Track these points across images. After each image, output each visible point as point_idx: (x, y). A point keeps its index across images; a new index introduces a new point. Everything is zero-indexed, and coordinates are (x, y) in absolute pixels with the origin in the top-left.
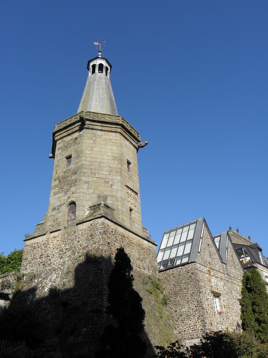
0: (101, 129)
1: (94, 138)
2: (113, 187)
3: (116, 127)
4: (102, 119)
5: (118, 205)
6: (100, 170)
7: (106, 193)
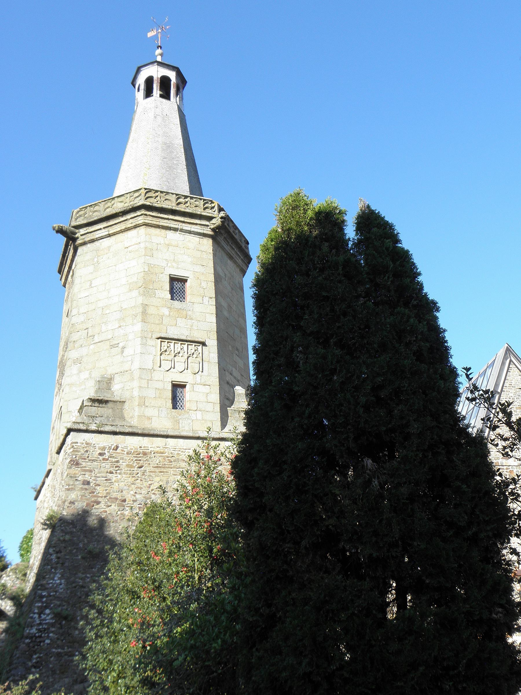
0: (107, 233)
1: (96, 260)
2: (126, 352)
3: (136, 215)
4: (108, 210)
5: (133, 389)
6: (103, 325)
7: (110, 371)
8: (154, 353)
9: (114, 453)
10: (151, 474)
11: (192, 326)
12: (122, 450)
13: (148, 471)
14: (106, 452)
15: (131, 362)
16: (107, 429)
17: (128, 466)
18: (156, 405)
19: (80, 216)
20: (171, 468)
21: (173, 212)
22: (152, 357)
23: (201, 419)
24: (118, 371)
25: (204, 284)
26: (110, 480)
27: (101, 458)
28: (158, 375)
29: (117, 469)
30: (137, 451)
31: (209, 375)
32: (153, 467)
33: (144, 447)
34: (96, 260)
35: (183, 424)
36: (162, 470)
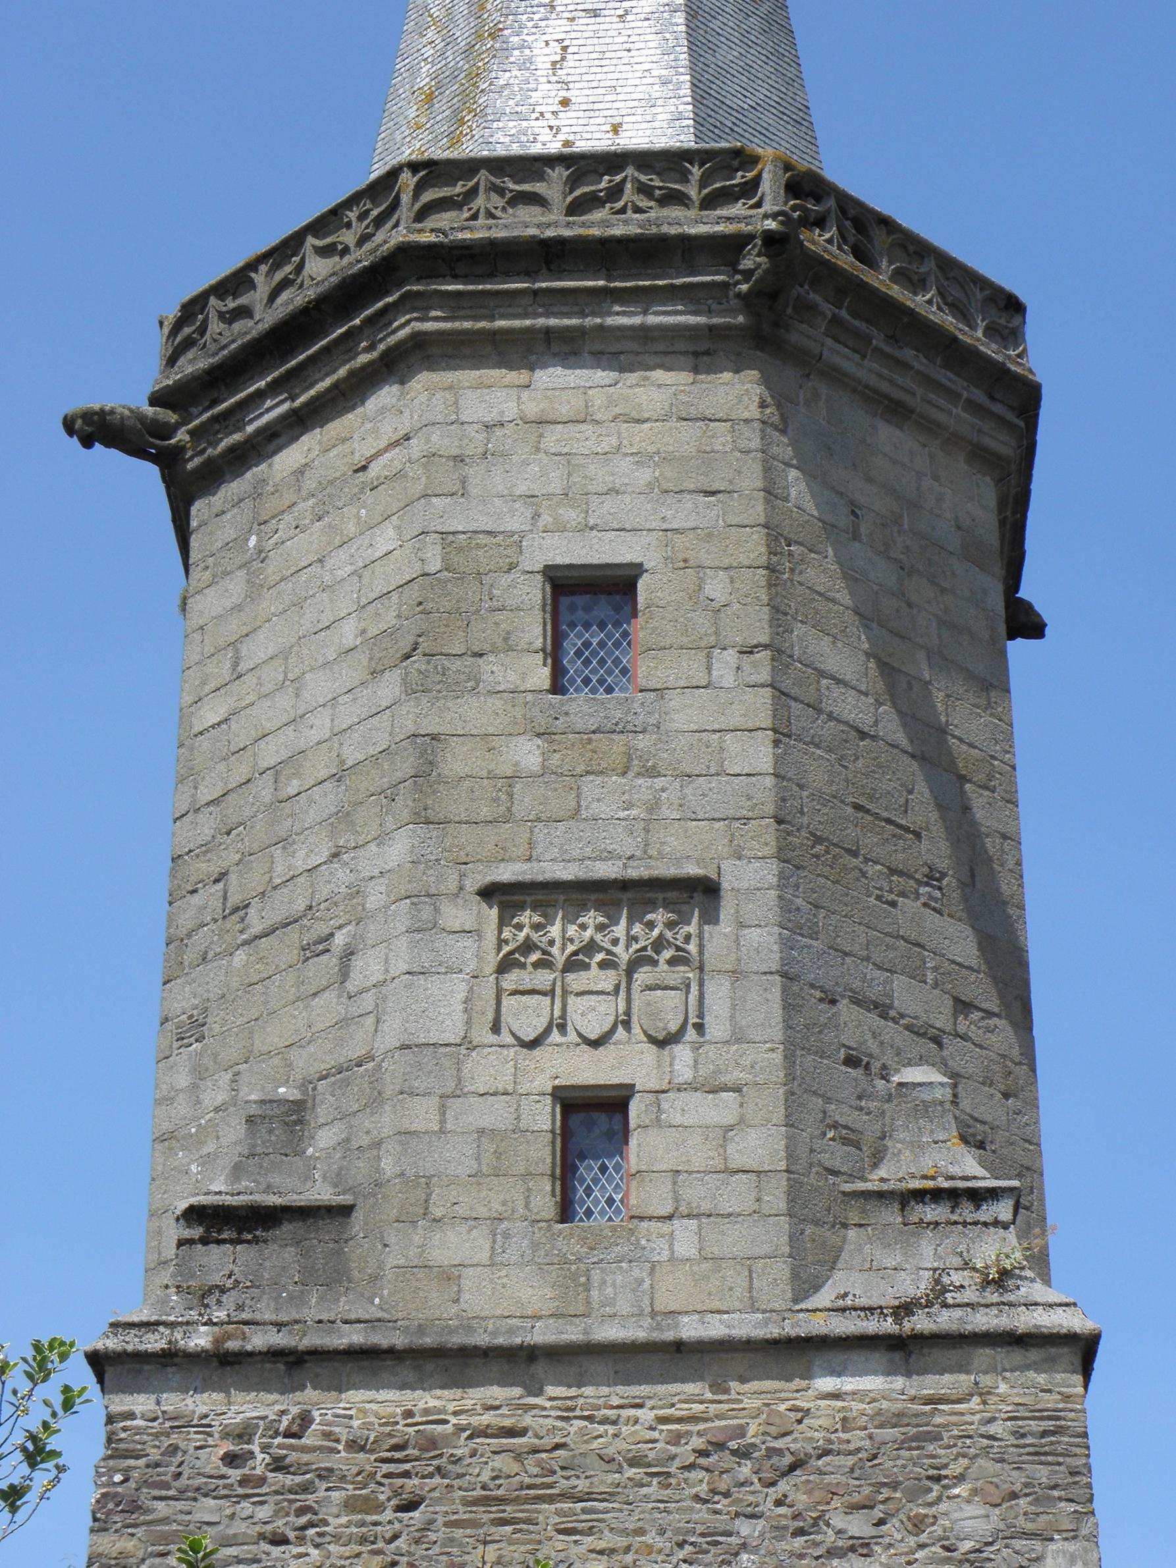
8: (472, 966)
9: (292, 1448)
10: (458, 1533)
11: (653, 806)
12: (327, 1435)
13: (441, 1519)
14: (256, 1448)
15: (370, 1020)
16: (258, 1341)
17: (350, 1505)
18: (482, 1212)
19: (188, 343)
20: (551, 1499)
21: (551, 254)
22: (458, 987)
23: (693, 1253)
24: (330, 1062)
25: (716, 588)
27: (235, 1474)
28: (491, 1067)
29: (303, 1520)
30: (390, 1435)
31: (738, 1037)
32: (467, 1503)
33: (426, 1412)
34: (253, 541)
35: (609, 1290)
36: (510, 1511)
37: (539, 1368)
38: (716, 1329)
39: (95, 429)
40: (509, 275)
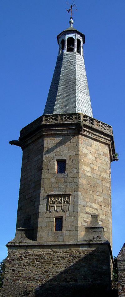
11: (66, 186)
26: (23, 268)
33: (40, 252)
36: (48, 262)
37: (52, 247)
38: (70, 243)
39: (12, 143)
40: (53, 128)
